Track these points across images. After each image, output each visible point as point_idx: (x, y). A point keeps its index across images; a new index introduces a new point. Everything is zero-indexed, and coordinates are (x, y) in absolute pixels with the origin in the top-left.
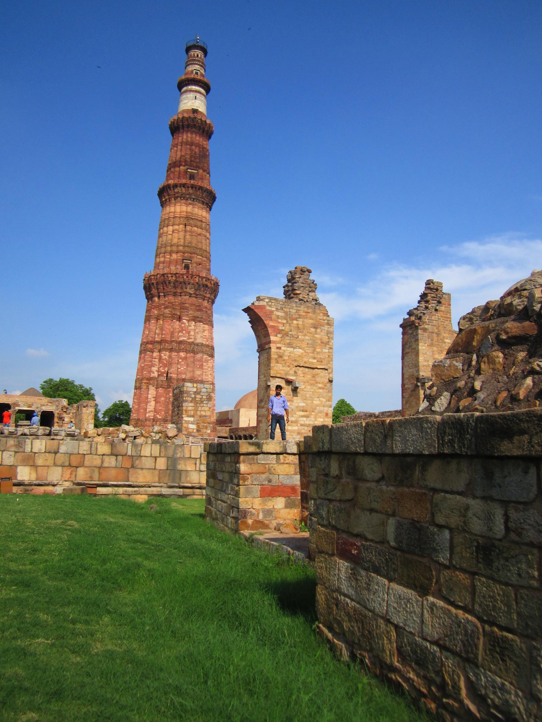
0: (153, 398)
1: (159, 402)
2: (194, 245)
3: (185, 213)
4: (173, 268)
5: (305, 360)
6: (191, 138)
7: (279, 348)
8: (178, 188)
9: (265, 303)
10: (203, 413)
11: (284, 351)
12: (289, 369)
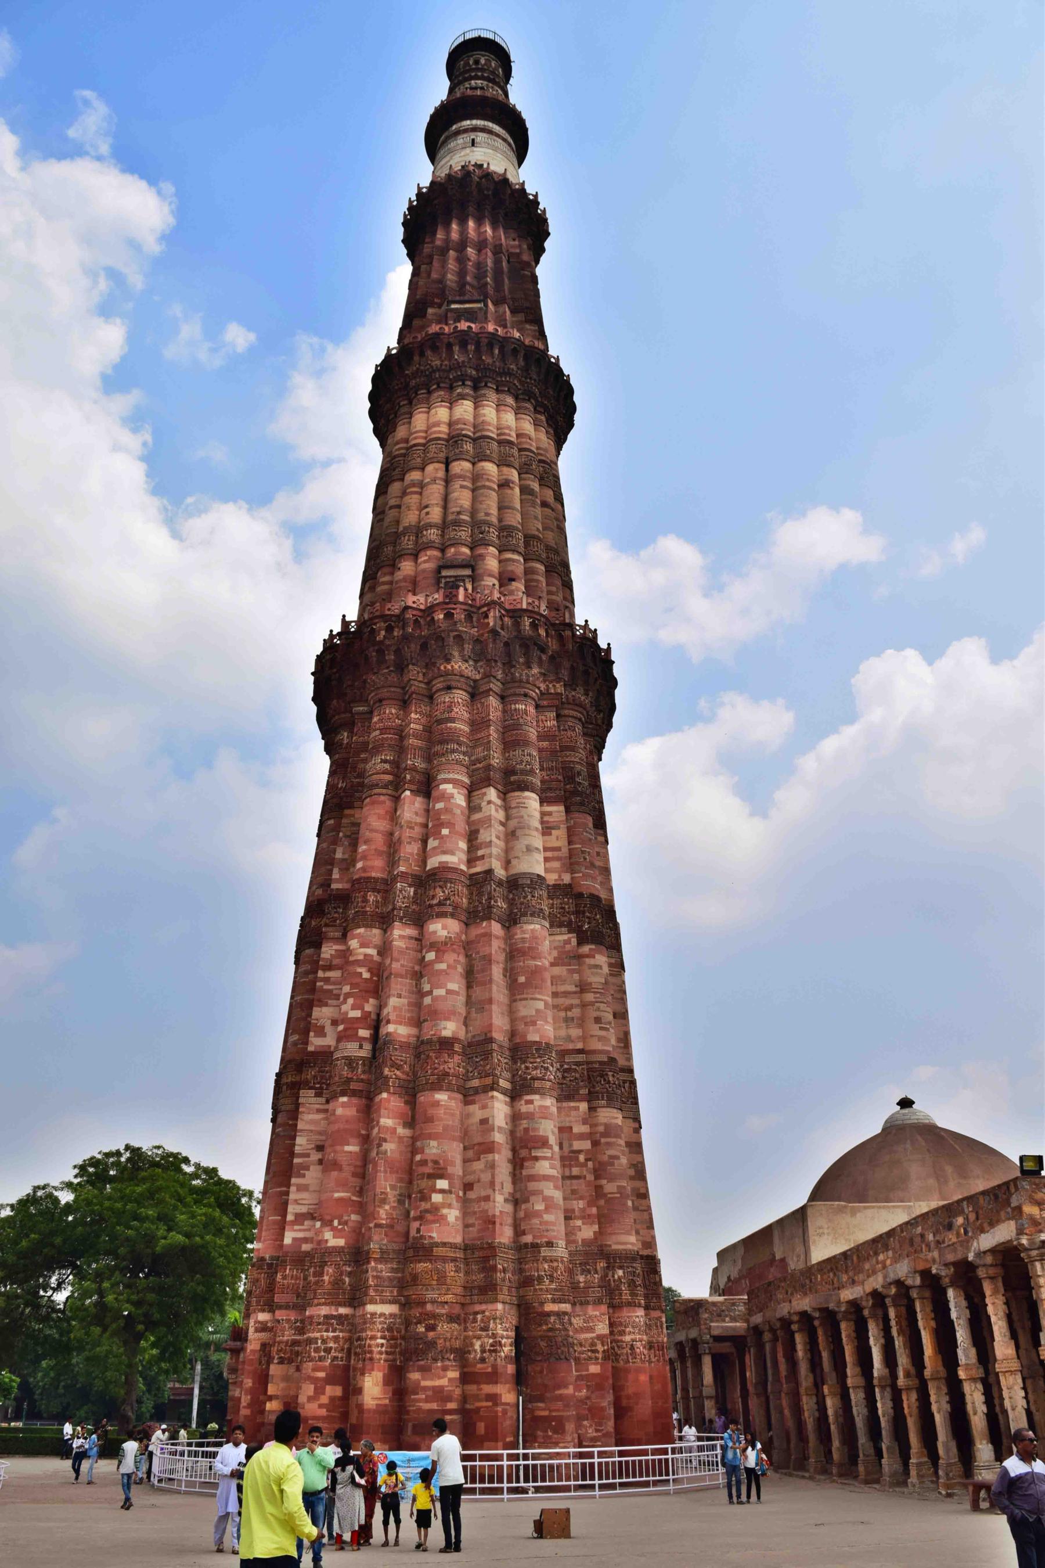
0: (320, 1148)
1: (336, 1165)
2: (481, 516)
3: (444, 429)
8: (416, 358)
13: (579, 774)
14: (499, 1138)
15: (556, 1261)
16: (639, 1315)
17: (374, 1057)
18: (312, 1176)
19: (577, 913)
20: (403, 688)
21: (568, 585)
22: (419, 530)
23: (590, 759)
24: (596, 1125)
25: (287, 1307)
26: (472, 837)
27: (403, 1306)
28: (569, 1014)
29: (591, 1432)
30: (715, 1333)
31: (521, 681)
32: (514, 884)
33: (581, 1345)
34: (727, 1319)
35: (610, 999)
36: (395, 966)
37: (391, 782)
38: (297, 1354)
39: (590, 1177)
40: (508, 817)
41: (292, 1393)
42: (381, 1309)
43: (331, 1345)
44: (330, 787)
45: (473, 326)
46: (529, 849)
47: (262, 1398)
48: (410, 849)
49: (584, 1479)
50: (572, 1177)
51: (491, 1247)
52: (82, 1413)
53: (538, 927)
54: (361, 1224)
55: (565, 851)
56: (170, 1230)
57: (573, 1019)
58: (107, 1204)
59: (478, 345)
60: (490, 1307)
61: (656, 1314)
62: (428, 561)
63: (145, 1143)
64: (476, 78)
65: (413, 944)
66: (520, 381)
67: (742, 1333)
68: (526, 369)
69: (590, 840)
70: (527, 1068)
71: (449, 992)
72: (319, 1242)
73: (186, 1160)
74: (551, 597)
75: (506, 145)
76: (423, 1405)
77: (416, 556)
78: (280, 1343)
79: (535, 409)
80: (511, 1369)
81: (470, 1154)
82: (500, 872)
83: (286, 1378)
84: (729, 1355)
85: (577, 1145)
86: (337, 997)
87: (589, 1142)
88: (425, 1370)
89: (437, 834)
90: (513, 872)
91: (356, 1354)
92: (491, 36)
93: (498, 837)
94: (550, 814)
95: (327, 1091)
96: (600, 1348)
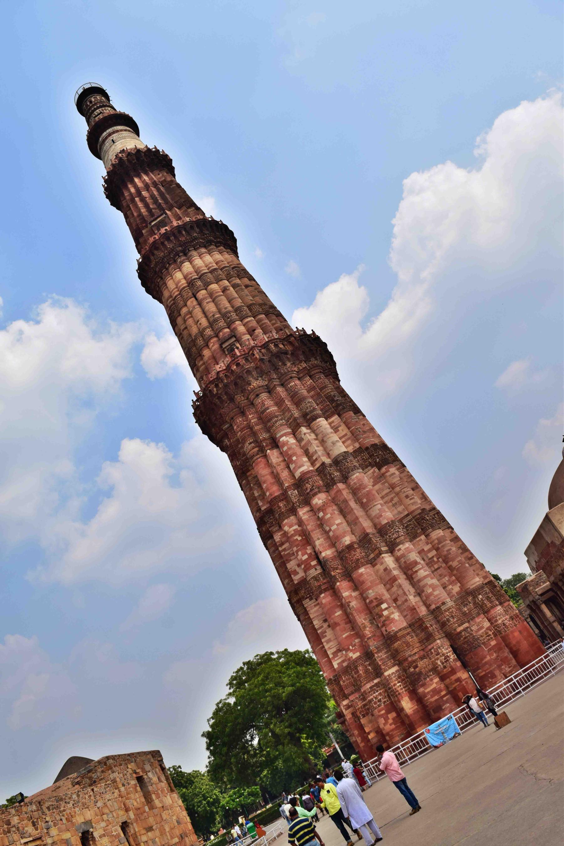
0: (325, 621)
1: (336, 624)
2: (224, 311)
3: (184, 281)
8: (152, 258)
13: (334, 396)
14: (396, 573)
15: (450, 608)
16: (499, 609)
17: (324, 570)
18: (329, 634)
19: (371, 456)
20: (238, 407)
21: (279, 315)
22: (201, 333)
23: (335, 385)
24: (433, 541)
25: (352, 693)
26: (307, 453)
27: (399, 665)
28: (393, 502)
29: (508, 669)
30: (540, 593)
31: (285, 373)
32: (336, 462)
33: (482, 636)
34: (542, 584)
35: (406, 484)
36: (309, 527)
37: (259, 451)
38: (368, 709)
39: (444, 565)
40: (317, 435)
41: (376, 726)
42: (391, 671)
43: (380, 698)
44: (235, 467)
45: (167, 228)
46: (334, 443)
47: (365, 735)
48: (284, 474)
49: (514, 691)
50: (436, 570)
51: (420, 619)
52: (293, 784)
53: (358, 474)
54: (362, 640)
55: (349, 434)
56: (284, 687)
57: (396, 503)
58: (251, 693)
59: (174, 235)
60: (434, 644)
61: (506, 604)
62: (214, 344)
63: (251, 657)
64: (95, 109)
65: (311, 513)
66: (202, 239)
67: (550, 587)
68: (201, 232)
69: (357, 421)
70: (390, 536)
71: (338, 525)
72: (349, 659)
73: (272, 653)
74: (275, 326)
75: (127, 132)
76: (432, 699)
77: (207, 346)
78: (358, 709)
79: (216, 246)
80: (459, 664)
81: (388, 586)
82: (328, 461)
83: (370, 721)
84: (551, 597)
85: (430, 555)
86: (293, 554)
87: (434, 551)
88: (423, 685)
89: (292, 462)
90: (333, 457)
91: (392, 695)
92: (90, 86)
93: (318, 447)
94: (333, 422)
95: (314, 595)
96: (490, 633)
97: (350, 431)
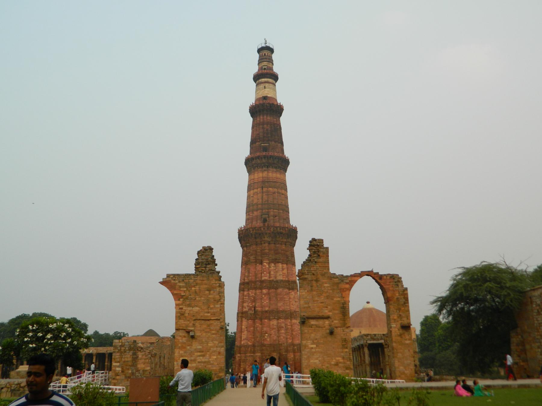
2: (269, 202)
3: (261, 179)
4: (254, 223)
5: (202, 314)
6: (263, 119)
7: (182, 309)
9: (170, 279)
10: (126, 360)
11: (185, 310)
12: (188, 322)
27: (262, 353)
32: (277, 281)
46: (280, 275)
59: (268, 158)
82: (275, 280)
97: (288, 273)
